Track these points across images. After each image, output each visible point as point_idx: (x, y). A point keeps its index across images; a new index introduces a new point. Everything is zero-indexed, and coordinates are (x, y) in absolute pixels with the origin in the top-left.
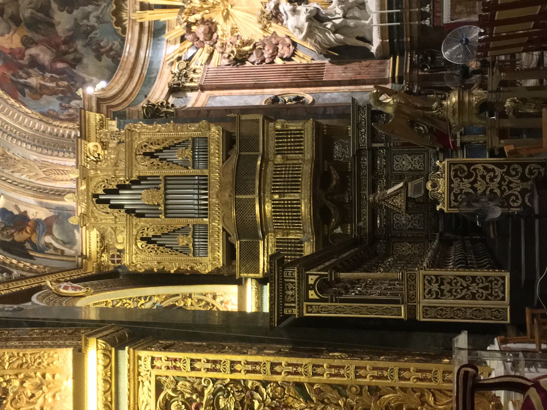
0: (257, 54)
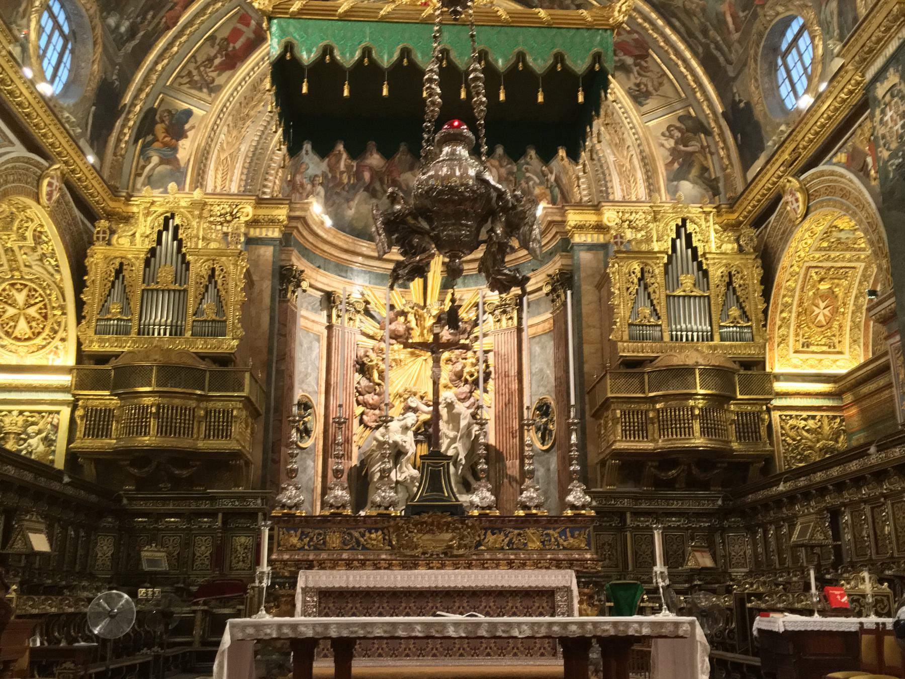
0: (368, 387)
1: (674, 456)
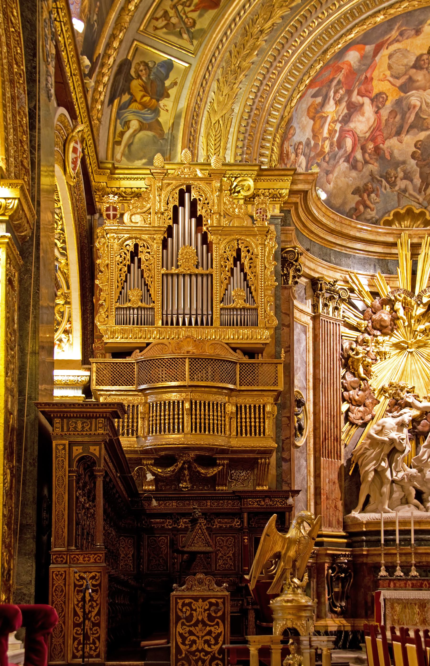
0: (353, 382)
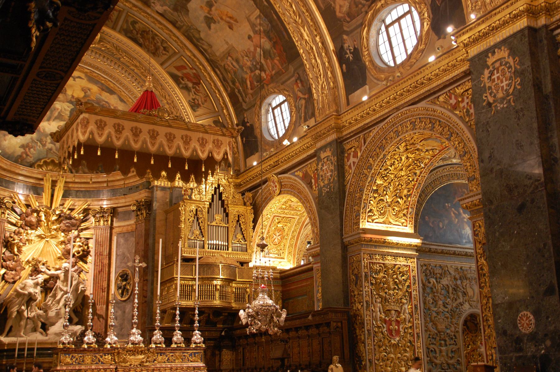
0: (10, 256)
1: (203, 309)
